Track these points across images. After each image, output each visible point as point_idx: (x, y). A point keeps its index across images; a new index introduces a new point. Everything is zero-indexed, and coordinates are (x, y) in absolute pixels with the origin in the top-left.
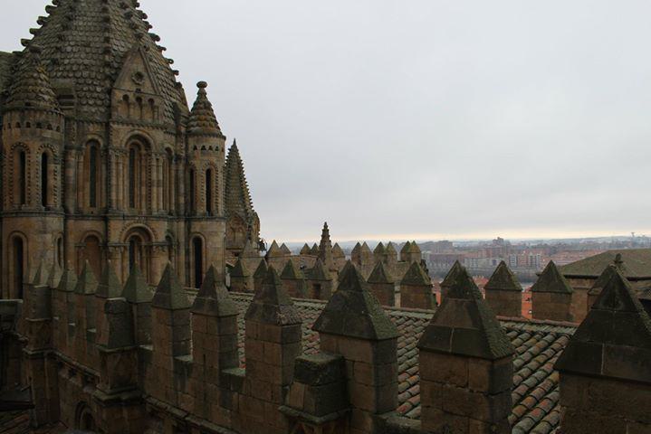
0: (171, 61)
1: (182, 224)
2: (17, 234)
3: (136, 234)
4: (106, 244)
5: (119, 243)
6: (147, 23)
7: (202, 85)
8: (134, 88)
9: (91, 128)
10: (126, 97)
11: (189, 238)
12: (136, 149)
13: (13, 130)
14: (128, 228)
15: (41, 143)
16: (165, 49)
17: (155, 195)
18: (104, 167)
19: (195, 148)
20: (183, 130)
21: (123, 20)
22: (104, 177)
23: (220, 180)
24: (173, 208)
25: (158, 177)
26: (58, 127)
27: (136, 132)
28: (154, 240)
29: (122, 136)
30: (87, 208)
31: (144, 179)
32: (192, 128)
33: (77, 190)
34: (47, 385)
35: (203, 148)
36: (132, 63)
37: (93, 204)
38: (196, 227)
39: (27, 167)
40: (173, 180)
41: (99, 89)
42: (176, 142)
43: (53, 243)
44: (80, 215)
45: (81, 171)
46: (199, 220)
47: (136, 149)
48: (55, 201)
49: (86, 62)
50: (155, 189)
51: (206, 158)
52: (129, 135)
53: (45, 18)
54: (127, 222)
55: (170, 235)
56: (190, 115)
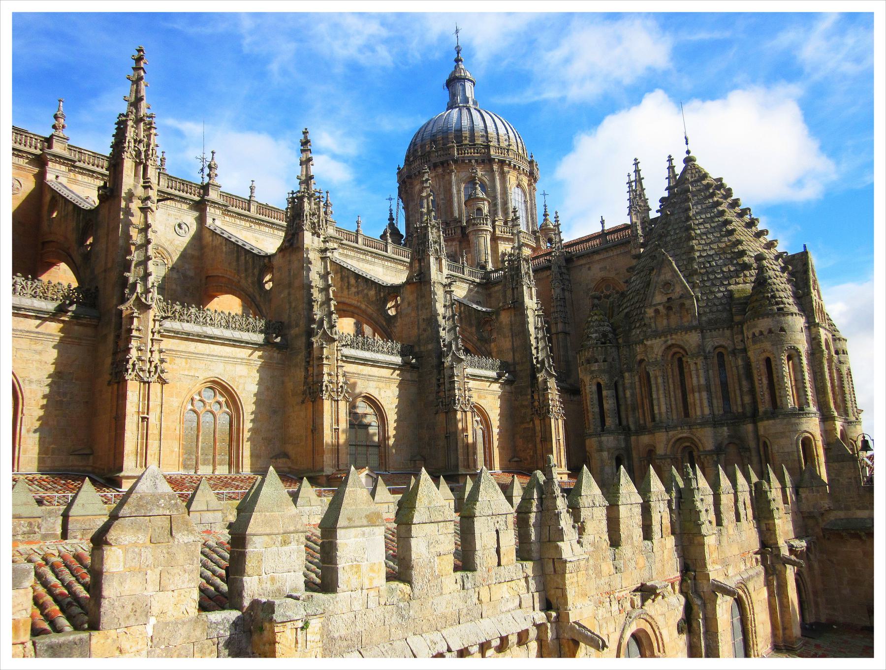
3: (688, 444)
5: (665, 455)
8: (665, 299)
10: (657, 311)
14: (673, 440)
24: (740, 410)
25: (699, 381)
26: (605, 358)
27: (669, 343)
29: (656, 350)
35: (754, 334)
36: (659, 275)
44: (642, 430)
46: (762, 420)
48: (610, 422)
50: (697, 395)
51: (757, 346)
52: (663, 348)
54: (671, 433)
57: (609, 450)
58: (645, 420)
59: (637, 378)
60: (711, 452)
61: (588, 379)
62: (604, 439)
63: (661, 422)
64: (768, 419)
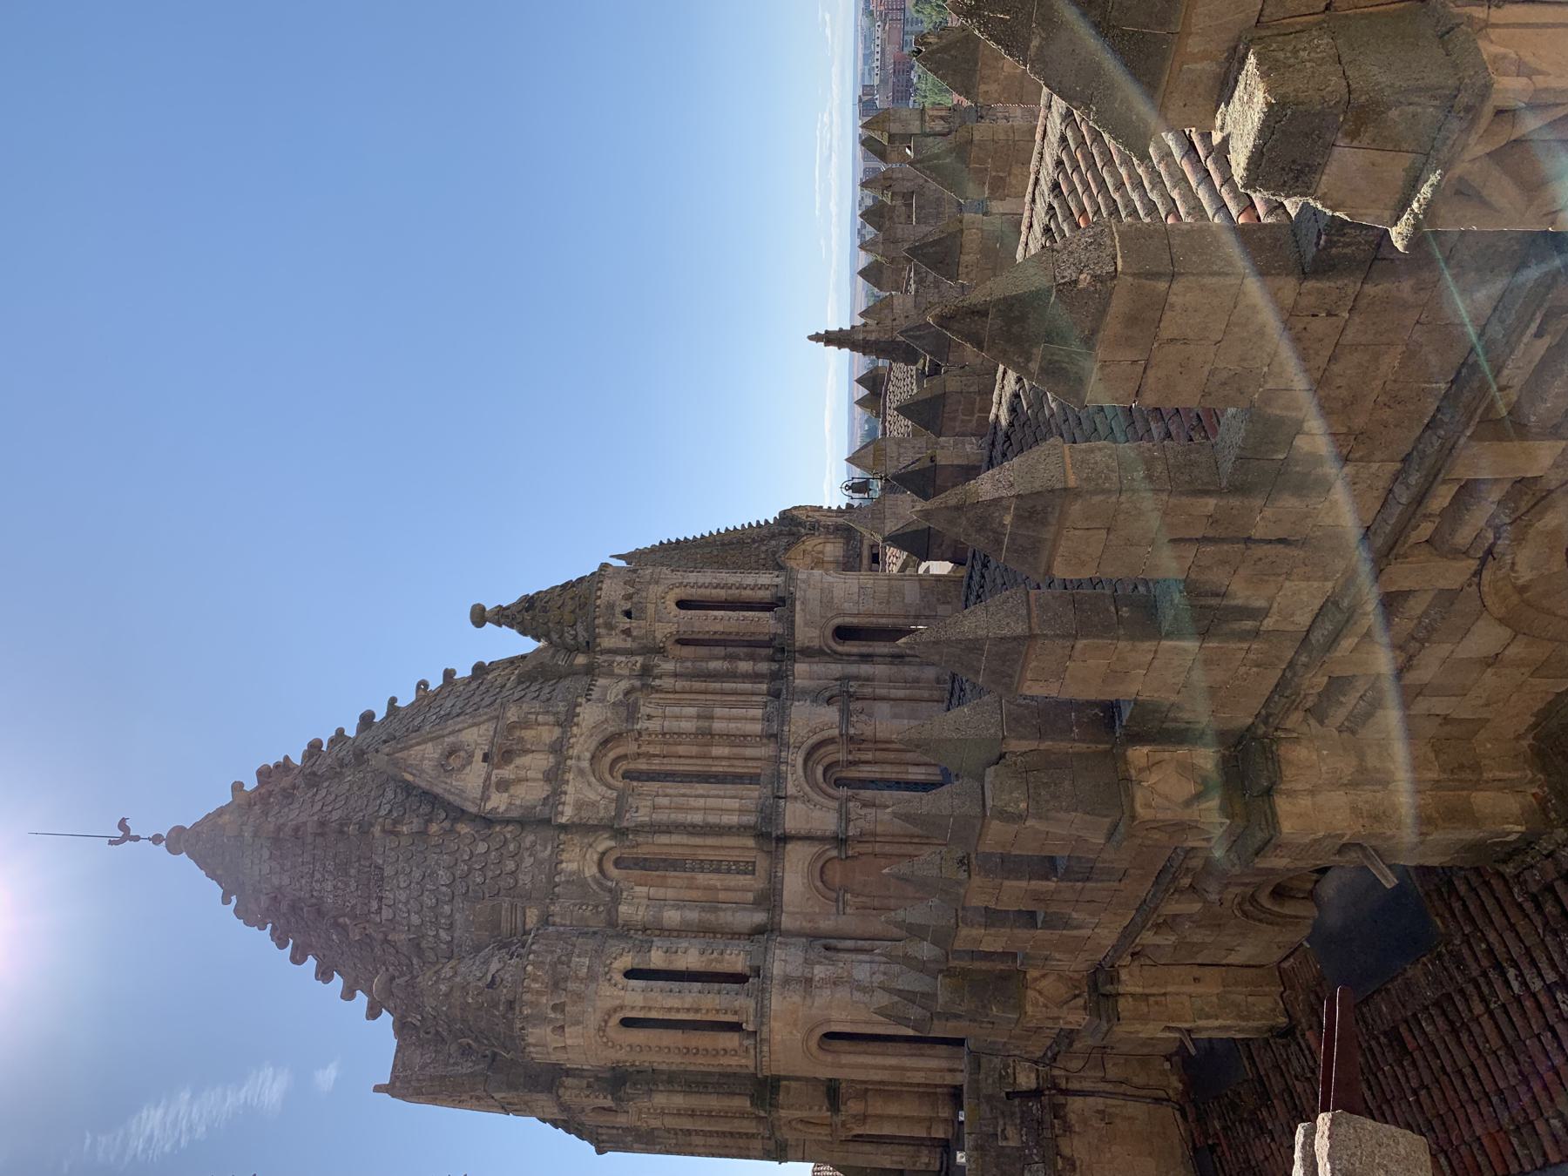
0: (422, 685)
1: (801, 668)
2: (813, 1043)
3: (820, 770)
4: (840, 841)
5: (839, 811)
6: (331, 741)
7: (480, 617)
9: (569, 866)
10: (503, 785)
11: (835, 652)
12: (623, 766)
13: (569, 1042)
15: (601, 979)
16: (393, 700)
17: (732, 725)
18: (664, 839)
19: (627, 632)
20: (581, 660)
21: (323, 792)
22: (684, 839)
23: (705, 581)
24: (764, 687)
27: (585, 764)
28: (836, 732)
29: (592, 796)
30: (756, 883)
31: (694, 750)
32: (580, 639)
33: (713, 906)
34: (1184, 989)
36: (422, 771)
37: (749, 869)
38: (806, 634)
39: (653, 1015)
40: (698, 685)
41: (482, 847)
42: (611, 674)
43: (833, 962)
44: (770, 898)
45: (671, 893)
47: (623, 766)
49: (417, 874)
50: (718, 726)
51: (651, 609)
52: (593, 779)
53: (319, 966)
54: (791, 790)
55: (827, 694)
56: (551, 642)
57: (807, 962)
58: (745, 890)
59: (641, 890)
60: (846, 714)
61: (606, 989)
62: (777, 969)
63: (761, 811)
64: (793, 611)
